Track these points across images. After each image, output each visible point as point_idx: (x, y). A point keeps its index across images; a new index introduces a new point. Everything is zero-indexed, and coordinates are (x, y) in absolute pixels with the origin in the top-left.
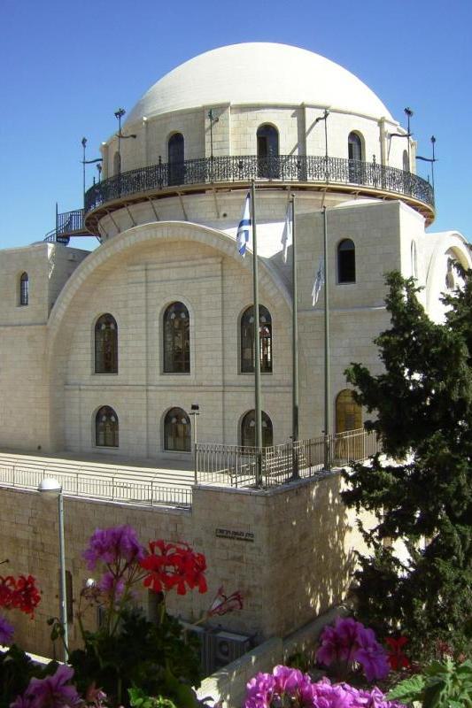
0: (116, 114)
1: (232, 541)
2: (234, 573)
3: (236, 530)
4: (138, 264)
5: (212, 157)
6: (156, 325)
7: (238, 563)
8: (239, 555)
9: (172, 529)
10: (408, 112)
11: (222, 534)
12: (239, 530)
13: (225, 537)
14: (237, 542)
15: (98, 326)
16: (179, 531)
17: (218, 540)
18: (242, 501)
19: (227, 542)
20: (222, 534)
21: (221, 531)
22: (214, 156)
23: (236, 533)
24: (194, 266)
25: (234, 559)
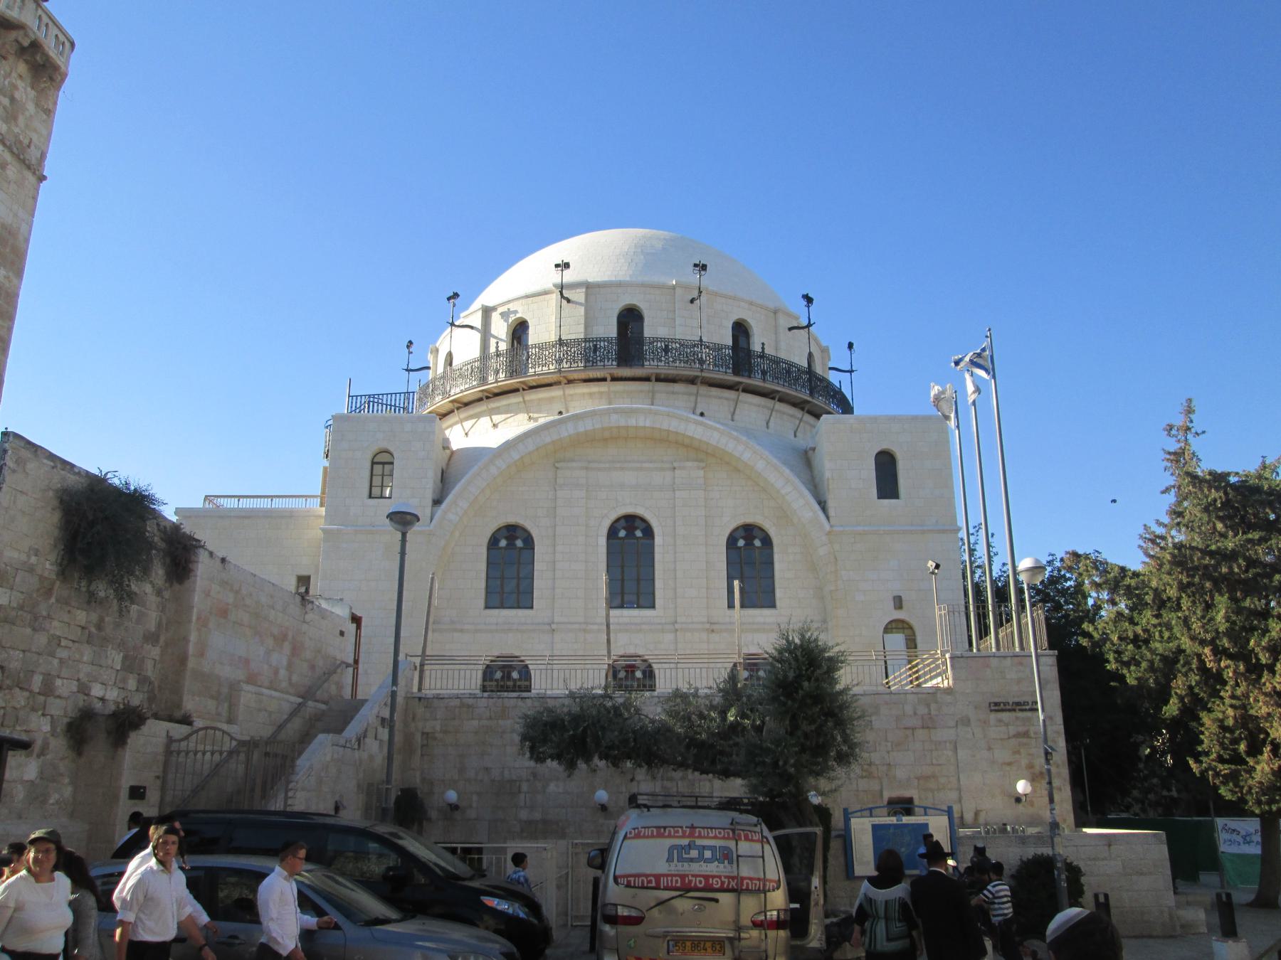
0: (557, 266)
1: (1013, 714)
2: (1018, 752)
3: (1016, 700)
4: (572, 460)
5: (701, 340)
6: (603, 541)
7: (1025, 740)
8: (1021, 729)
9: (922, 710)
10: (850, 346)
11: (997, 707)
12: (1021, 700)
13: (1002, 710)
14: (1020, 714)
15: (493, 542)
16: (933, 713)
17: (993, 716)
18: (1021, 664)
19: (1005, 716)
20: (997, 707)
21: (996, 704)
22: (704, 339)
23: (1018, 704)
24: (662, 469)
25: (1018, 735)
